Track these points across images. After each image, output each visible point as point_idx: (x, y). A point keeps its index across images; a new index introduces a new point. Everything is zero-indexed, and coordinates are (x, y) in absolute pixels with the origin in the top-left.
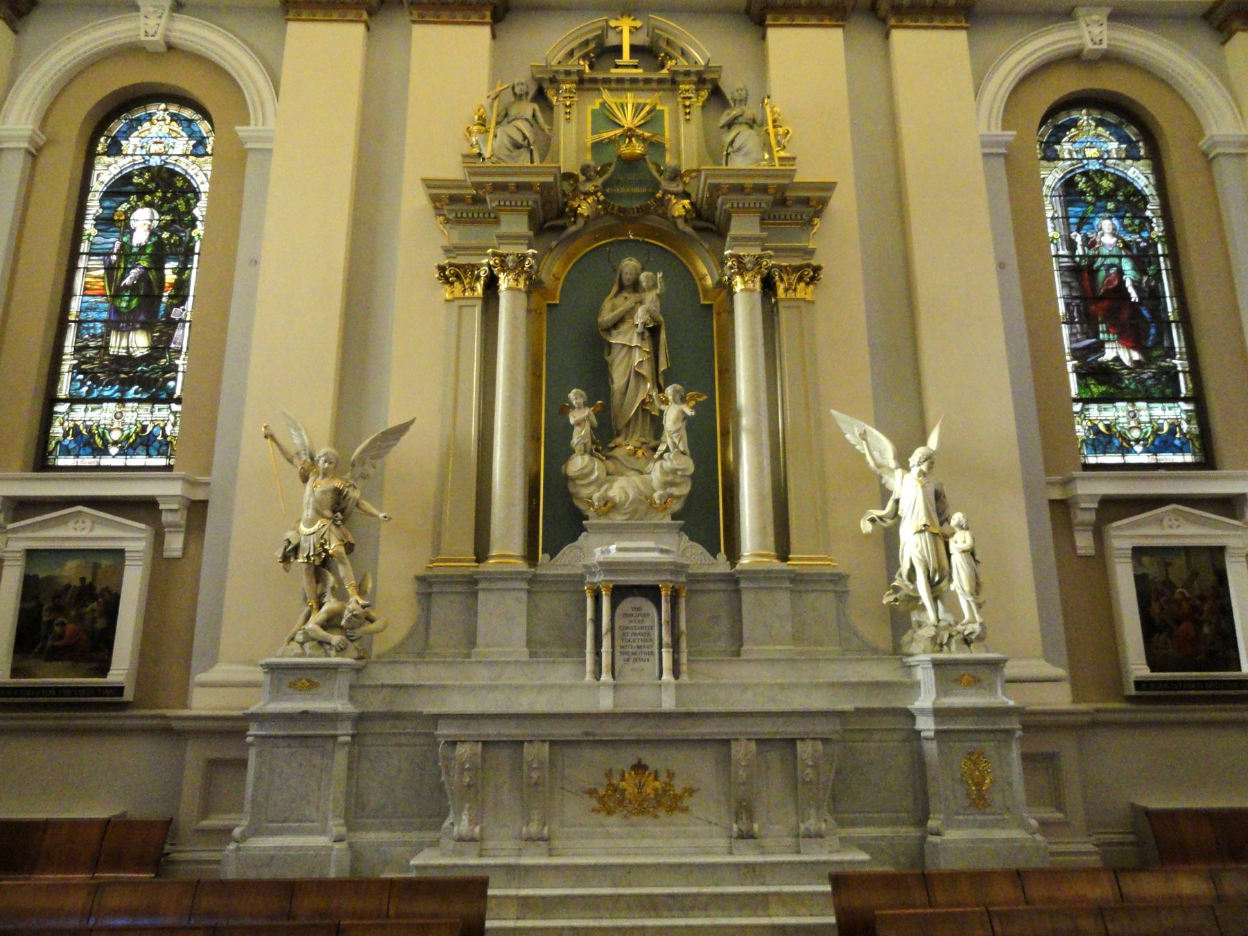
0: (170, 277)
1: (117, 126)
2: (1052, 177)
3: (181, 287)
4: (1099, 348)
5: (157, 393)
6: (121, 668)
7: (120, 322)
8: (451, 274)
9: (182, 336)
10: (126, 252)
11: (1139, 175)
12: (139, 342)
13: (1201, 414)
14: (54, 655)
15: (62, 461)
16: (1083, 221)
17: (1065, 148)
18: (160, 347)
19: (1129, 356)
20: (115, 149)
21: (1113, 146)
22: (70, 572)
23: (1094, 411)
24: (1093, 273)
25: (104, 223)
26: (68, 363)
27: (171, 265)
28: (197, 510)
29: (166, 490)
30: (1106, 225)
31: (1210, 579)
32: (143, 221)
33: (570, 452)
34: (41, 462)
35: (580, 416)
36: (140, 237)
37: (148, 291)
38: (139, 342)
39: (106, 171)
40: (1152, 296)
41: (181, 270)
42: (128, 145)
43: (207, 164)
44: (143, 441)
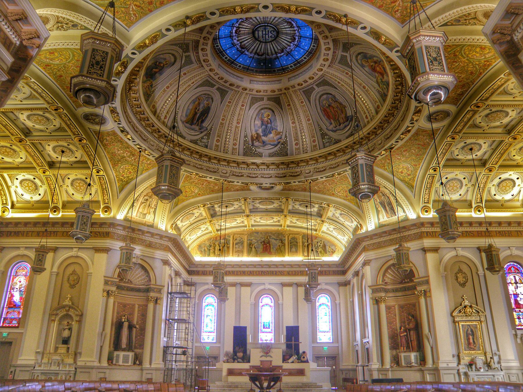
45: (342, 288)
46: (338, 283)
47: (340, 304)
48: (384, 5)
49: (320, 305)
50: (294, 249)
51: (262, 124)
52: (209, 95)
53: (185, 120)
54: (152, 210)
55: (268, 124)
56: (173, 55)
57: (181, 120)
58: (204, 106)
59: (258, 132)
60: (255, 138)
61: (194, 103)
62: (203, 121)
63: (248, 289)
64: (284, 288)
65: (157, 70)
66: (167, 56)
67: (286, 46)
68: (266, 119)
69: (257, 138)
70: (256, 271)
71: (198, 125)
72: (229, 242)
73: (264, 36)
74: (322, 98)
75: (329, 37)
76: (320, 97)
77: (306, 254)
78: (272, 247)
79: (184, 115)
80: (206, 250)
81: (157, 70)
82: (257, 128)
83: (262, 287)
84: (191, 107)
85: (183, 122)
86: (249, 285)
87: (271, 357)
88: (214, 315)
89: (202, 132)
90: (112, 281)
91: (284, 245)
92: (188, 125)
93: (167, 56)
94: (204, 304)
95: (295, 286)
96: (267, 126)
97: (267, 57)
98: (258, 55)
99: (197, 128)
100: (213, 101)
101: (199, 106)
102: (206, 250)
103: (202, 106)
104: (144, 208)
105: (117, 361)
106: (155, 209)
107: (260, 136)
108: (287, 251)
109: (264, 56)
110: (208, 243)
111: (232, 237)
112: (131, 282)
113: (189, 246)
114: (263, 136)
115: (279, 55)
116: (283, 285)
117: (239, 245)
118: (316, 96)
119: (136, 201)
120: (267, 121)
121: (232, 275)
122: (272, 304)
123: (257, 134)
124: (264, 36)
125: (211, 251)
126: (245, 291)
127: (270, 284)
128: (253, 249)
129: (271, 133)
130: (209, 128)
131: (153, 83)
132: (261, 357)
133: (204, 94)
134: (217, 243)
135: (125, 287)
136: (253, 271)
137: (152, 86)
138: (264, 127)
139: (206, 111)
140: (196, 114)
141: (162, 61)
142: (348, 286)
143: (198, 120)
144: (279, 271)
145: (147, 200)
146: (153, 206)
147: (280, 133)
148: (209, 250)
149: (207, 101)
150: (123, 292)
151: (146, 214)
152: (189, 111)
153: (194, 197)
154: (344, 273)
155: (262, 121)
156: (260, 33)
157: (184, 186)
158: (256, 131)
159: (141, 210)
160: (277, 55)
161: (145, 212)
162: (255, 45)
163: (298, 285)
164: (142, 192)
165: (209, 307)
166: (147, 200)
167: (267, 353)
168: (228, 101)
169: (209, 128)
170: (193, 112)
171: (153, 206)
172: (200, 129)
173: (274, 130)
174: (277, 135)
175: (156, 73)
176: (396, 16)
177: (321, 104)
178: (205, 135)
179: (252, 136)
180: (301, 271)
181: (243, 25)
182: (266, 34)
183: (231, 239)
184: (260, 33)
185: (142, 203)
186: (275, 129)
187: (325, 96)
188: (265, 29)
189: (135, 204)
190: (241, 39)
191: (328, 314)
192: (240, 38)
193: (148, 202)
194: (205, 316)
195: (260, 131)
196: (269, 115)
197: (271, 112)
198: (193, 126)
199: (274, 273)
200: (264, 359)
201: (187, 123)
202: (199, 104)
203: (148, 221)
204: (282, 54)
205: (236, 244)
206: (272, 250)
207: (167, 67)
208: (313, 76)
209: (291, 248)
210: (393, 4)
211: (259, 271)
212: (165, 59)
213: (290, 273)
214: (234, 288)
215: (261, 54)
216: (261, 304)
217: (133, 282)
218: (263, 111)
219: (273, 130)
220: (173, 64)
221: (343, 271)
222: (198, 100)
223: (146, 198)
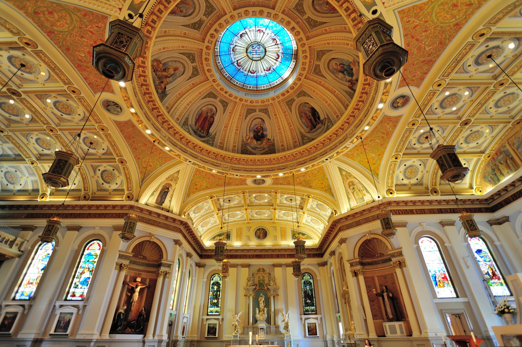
0: (218, 294)
1: (213, 277)
2: (303, 281)
3: (219, 295)
4: (307, 301)
5: (218, 307)
6: (217, 336)
7: (214, 299)
8: (245, 296)
9: (220, 300)
10: (214, 291)
11: (311, 281)
12: (215, 301)
13: (316, 308)
14: (211, 334)
15: (210, 314)
16: (306, 286)
17: (304, 278)
18: (218, 301)
19: (310, 301)
20: (213, 280)
21: (309, 277)
22: (212, 326)
23: (306, 307)
24: (306, 292)
25: (212, 288)
26: (209, 303)
27: (218, 293)
28: (223, 319)
29: (220, 317)
30: (308, 287)
31: (315, 326)
32: (216, 287)
33: (256, 314)
34: (208, 315)
35: (257, 311)
36: (215, 289)
37: (216, 295)
38: (215, 301)
39: (212, 282)
40: (312, 295)
41: (219, 293)
42: (214, 279)
43: (221, 281)
44: (217, 312)
48: (99, 38)
51: (343, 72)
52: (301, 104)
53: (309, 130)
54: (364, 192)
55: (344, 68)
56: (255, 119)
57: (307, 133)
58: (309, 111)
59: (348, 80)
60: (351, 86)
61: (302, 117)
62: (319, 118)
65: (261, 132)
66: (254, 123)
67: (268, 36)
68: (339, 67)
69: (352, 84)
71: (319, 123)
72: (509, 152)
73: (257, 53)
74: (320, 11)
75: (231, 14)
76: (318, 11)
79: (306, 128)
80: (492, 176)
81: (261, 132)
82: (345, 79)
84: (304, 121)
85: (309, 132)
89: (325, 124)
90: (355, 262)
92: (313, 130)
93: (254, 123)
96: (345, 70)
97: (281, 51)
98: (278, 58)
99: (320, 125)
100: (308, 103)
101: (307, 114)
102: (492, 176)
103: (308, 113)
104: (358, 195)
105: (387, 333)
106: (366, 189)
107: (352, 80)
109: (280, 55)
110: (489, 170)
111: (507, 145)
112: (383, 254)
114: (352, 78)
115: (278, 42)
118: (317, 16)
119: (348, 195)
120: (342, 67)
123: (349, 81)
124: (257, 53)
125: (498, 174)
129: (352, 69)
130: (326, 117)
131: (268, 137)
133: (299, 107)
134: (497, 163)
135: (379, 261)
137: (269, 139)
138: (345, 72)
139: (314, 111)
140: (310, 120)
141: (256, 127)
143: (316, 121)
145: (354, 188)
146: (362, 189)
147: (354, 61)
148: (495, 174)
149: (306, 107)
150: (379, 266)
151: (363, 197)
152: (306, 123)
153: (380, 160)
155: (340, 72)
156: (255, 56)
157: (360, 161)
158: (346, 81)
159: (357, 197)
160: (278, 44)
161: (361, 197)
162: (269, 60)
164: (345, 186)
166: (354, 188)
168: (312, 92)
169: (326, 117)
170: (308, 121)
171: (362, 189)
172: (322, 123)
173: (351, 65)
174: (355, 65)
175: (262, 134)
176: (103, 25)
177: (327, 12)
178: (328, 123)
179: (349, 87)
181: (247, 68)
182: (256, 52)
183: (508, 147)
184: (255, 56)
185: (353, 193)
186: (350, 64)
187: (317, 7)
188: (250, 53)
189: (350, 197)
190: (261, 70)
192: (260, 71)
193: (356, 189)
195: (349, 78)
196: (336, 64)
197: (333, 60)
198: (317, 127)
201: (312, 130)
202: (305, 114)
203: (368, 201)
204: (277, 39)
207: (263, 125)
208: (285, 22)
210: (94, 32)
212: (256, 125)
215: (277, 57)
217: (385, 254)
218: (330, 68)
219: (350, 66)
220: (263, 120)
222: (301, 114)
223: (351, 187)
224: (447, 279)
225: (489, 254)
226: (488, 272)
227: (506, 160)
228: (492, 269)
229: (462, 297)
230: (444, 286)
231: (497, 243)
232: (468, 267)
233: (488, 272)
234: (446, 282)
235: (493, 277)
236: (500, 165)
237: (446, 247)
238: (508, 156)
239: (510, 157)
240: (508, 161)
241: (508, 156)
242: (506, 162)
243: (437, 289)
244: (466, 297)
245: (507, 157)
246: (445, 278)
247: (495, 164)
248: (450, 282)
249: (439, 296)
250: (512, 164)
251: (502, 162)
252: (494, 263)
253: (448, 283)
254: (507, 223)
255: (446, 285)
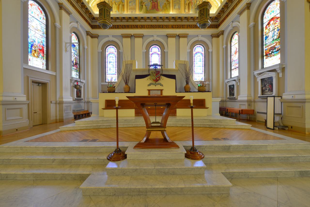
45: (214, 39)
46: (211, 35)
47: (212, 52)
49: (196, 53)
50: (177, 7)
63: (141, 39)
64: (169, 39)
70: (147, 25)
77: (187, 11)
78: (159, 4)
83: (151, 39)
86: (141, 36)
87: (162, 85)
88: (115, 61)
91: (169, 4)
94: (107, 53)
95: (177, 38)
108: (171, 8)
113: (88, 3)
116: (168, 36)
117: (132, 3)
121: (127, 28)
122: (160, 53)
126: (138, 41)
127: (158, 36)
128: (144, 7)
132: (149, 85)
136: (144, 25)
142: (221, 37)
144: (165, 25)
154: (217, 26)
163: (179, 36)
165: (110, 55)
167: (157, 80)
180: (182, 25)
191: (202, 60)
194: (108, 63)
199: (161, 26)
200: (152, 87)
205: (130, 2)
206: (159, 8)
209: (175, 6)
211: (149, 25)
213: (174, 27)
214: (129, 39)
216: (151, 53)
221: (216, 25)
224: (43, 52)
225: (78, 51)
226: (73, 61)
227: (120, 4)
228: (76, 61)
229: (52, 70)
230: (38, 57)
231: (86, 47)
232: (66, 51)
233: (73, 61)
234: (41, 54)
235: (74, 65)
236: (114, 4)
237: (55, 27)
238: (123, 3)
239: (123, 4)
240: (120, 5)
241: (123, 3)
242: (119, 5)
243: (30, 57)
244: (56, 71)
245: (121, 3)
246: (42, 50)
247: (112, 2)
248: (45, 56)
249: (30, 64)
250: (121, 8)
251: (117, 3)
252: (78, 57)
253: (43, 56)
254: (96, 39)
255: (40, 56)
